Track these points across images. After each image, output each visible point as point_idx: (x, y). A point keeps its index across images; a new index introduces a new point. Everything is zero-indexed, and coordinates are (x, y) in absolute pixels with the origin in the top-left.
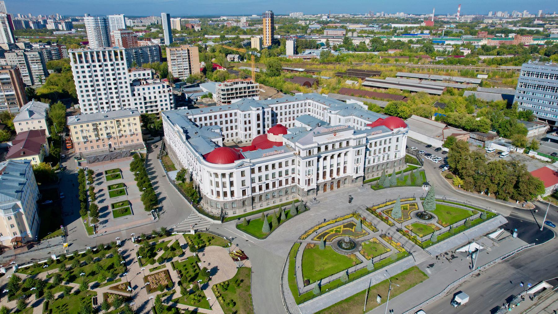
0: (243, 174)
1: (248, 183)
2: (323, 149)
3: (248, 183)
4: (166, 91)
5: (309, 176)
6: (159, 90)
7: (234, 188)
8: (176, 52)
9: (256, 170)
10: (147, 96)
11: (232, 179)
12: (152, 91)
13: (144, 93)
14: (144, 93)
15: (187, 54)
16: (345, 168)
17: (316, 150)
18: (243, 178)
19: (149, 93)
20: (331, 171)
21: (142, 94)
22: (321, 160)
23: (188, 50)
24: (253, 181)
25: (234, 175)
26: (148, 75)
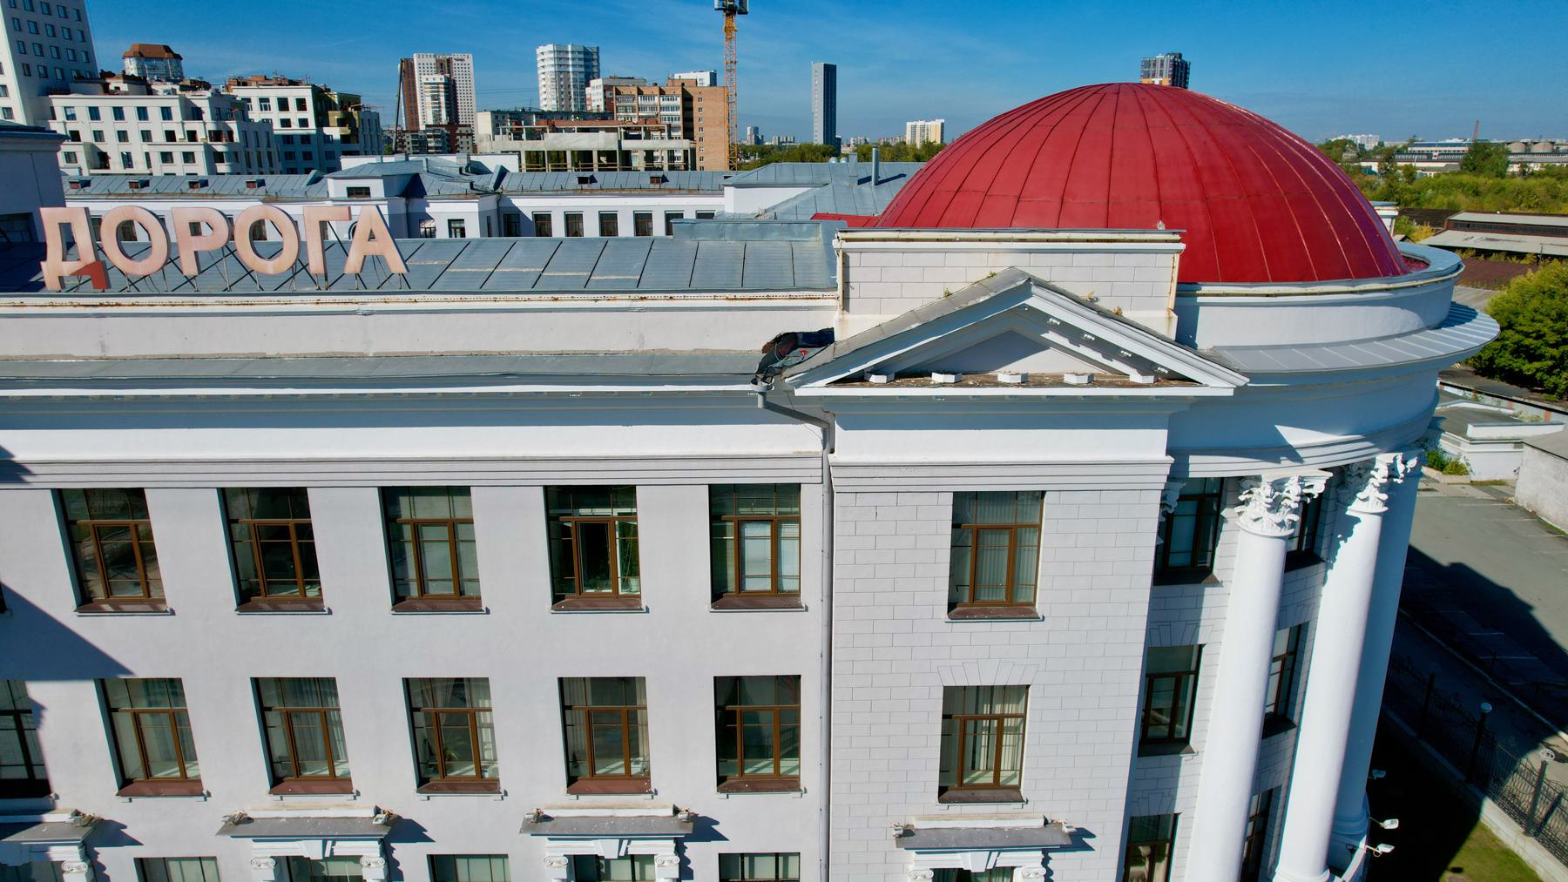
4: (201, 135)
6: (169, 126)
8: (641, 101)
10: (112, 147)
12: (132, 124)
13: (98, 135)
14: (98, 135)
15: (679, 113)
19: (123, 136)
21: (86, 137)
23: (687, 99)
26: (301, 104)
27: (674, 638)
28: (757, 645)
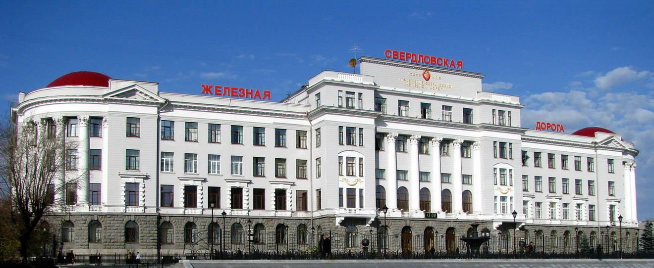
0: (132, 126)
1: (147, 163)
3: (147, 163)
5: (352, 180)
7: (101, 177)
9: (179, 130)
11: (95, 143)
16: (467, 197)
18: (132, 143)
20: (425, 195)
22: (389, 145)
24: (163, 161)
25: (105, 130)
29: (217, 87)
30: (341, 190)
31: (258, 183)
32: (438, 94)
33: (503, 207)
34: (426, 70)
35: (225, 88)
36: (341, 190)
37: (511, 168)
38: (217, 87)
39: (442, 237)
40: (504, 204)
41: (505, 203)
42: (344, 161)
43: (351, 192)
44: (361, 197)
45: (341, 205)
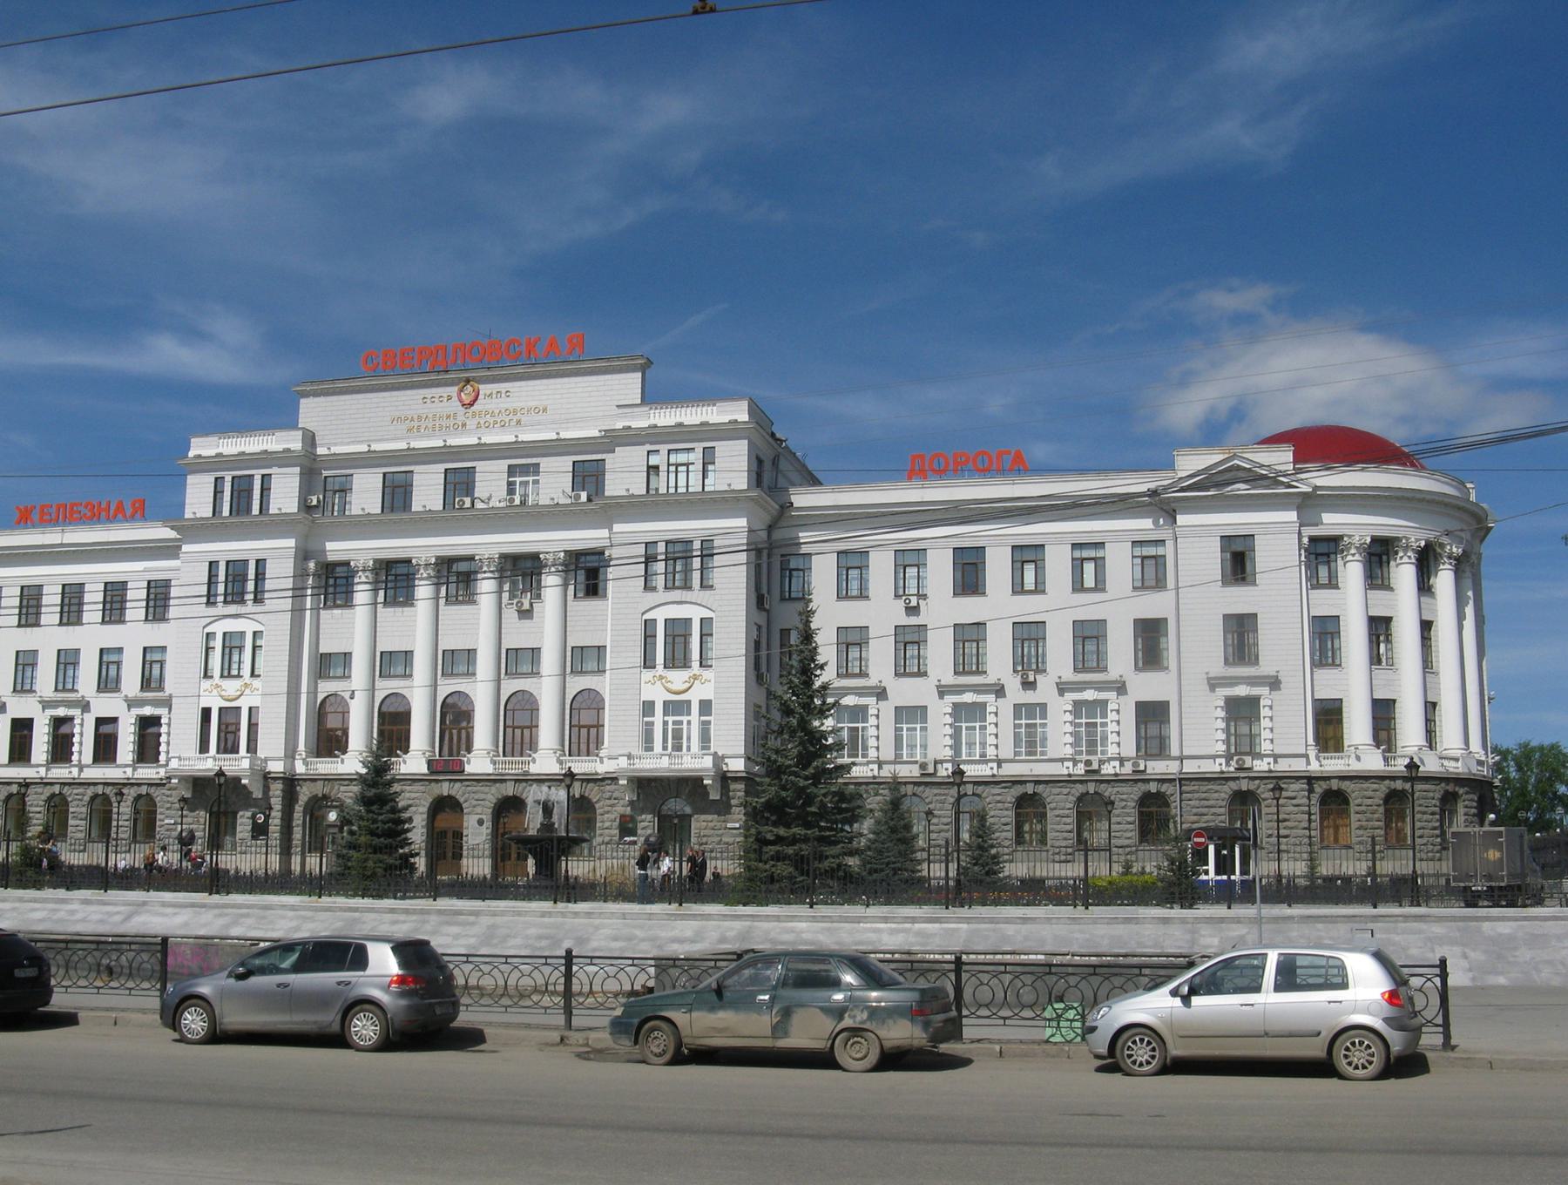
2: (366, 494)
5: (231, 687)
17: (285, 494)
27: (1120, 609)
28: (1154, 605)
29: (42, 508)
30: (206, 712)
31: (105, 706)
32: (490, 438)
33: (677, 735)
34: (468, 381)
35: (59, 507)
36: (206, 712)
37: (707, 614)
38: (42, 508)
39: (481, 822)
40: (681, 723)
41: (685, 719)
42: (218, 643)
43: (229, 716)
44: (253, 727)
45: (204, 747)
